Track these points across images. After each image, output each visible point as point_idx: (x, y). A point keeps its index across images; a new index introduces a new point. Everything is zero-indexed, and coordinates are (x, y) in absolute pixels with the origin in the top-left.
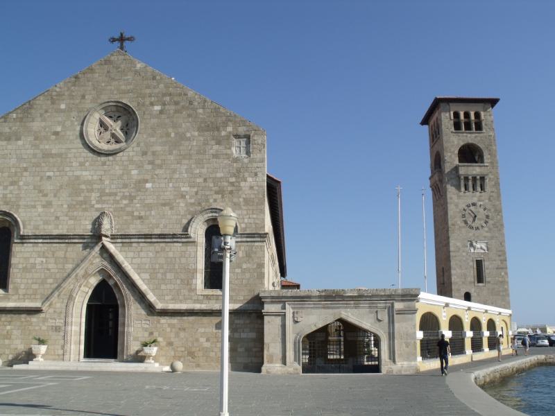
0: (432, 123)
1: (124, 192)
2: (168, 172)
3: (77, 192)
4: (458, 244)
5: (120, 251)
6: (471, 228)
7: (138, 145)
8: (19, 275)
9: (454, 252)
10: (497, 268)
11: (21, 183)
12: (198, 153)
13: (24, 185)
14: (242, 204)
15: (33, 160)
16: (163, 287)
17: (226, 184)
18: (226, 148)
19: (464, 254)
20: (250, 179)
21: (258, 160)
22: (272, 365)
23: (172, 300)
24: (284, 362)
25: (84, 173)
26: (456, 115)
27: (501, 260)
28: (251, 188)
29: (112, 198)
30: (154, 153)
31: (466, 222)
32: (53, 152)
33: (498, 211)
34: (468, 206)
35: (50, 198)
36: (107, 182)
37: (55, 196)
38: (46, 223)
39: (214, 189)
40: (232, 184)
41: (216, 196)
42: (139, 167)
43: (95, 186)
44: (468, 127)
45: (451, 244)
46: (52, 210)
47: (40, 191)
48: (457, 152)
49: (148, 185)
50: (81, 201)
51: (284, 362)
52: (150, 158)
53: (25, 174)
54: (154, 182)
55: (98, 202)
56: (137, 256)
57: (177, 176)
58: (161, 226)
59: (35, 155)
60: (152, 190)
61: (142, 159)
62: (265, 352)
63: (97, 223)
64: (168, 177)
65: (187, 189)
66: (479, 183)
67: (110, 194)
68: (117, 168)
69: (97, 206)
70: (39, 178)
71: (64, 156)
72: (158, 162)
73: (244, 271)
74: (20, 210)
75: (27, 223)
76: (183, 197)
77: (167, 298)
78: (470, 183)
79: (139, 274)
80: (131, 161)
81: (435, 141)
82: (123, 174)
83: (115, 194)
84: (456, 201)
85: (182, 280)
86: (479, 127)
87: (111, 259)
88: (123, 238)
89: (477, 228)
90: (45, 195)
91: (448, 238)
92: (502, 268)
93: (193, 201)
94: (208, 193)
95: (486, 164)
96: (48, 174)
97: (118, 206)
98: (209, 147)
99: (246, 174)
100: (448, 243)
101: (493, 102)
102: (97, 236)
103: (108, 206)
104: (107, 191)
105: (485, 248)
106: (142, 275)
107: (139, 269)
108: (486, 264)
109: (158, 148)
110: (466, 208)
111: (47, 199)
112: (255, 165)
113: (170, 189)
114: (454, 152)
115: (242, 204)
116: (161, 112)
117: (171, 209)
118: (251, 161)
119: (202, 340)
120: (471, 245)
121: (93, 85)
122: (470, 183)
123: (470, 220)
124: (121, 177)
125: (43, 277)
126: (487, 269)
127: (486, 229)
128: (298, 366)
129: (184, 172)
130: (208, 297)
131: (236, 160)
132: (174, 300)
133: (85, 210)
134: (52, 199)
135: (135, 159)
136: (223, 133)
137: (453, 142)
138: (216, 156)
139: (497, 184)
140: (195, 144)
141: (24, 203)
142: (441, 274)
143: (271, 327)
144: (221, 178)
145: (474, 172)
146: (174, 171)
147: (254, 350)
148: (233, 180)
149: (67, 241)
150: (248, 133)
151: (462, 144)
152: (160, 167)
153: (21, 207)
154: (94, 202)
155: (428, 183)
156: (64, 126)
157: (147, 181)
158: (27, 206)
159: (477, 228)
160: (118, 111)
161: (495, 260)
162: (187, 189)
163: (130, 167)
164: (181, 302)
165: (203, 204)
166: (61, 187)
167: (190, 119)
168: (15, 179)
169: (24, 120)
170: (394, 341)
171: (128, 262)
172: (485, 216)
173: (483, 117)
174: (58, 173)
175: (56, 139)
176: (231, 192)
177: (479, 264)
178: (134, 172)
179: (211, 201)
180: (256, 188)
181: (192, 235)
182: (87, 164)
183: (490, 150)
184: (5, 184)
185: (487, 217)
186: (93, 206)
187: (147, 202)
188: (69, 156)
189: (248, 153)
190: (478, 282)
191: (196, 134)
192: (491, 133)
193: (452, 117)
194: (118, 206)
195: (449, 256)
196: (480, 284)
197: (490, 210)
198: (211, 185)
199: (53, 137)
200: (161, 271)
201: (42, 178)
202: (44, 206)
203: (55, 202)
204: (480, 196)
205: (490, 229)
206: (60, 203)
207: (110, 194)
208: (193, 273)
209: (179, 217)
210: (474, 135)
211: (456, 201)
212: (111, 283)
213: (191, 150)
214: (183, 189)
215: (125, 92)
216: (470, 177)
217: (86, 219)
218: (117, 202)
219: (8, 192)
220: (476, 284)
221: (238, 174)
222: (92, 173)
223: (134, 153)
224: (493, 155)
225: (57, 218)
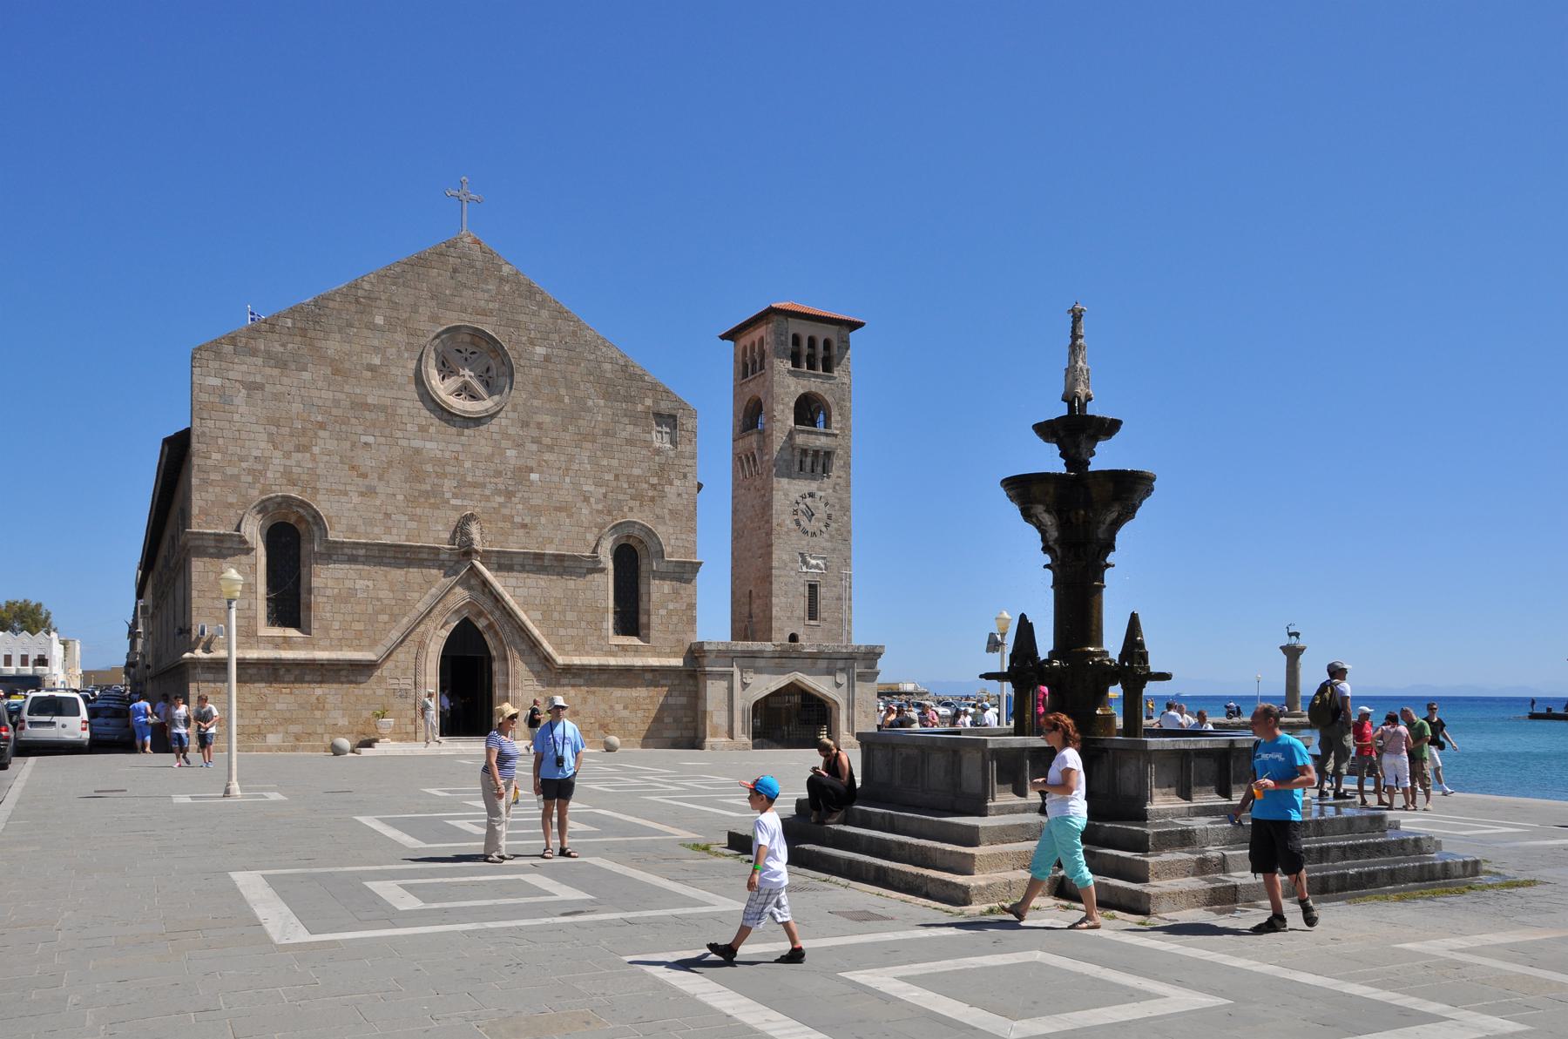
0: (746, 340)
1: (496, 484)
2: (562, 459)
3: (416, 476)
4: (785, 557)
5: (495, 577)
7: (514, 411)
8: (328, 608)
9: (778, 568)
11: (316, 450)
12: (606, 433)
13: (322, 453)
14: (667, 517)
15: (335, 411)
16: (562, 632)
17: (646, 486)
18: (644, 431)
19: (793, 573)
20: (677, 482)
21: (687, 454)
22: (716, 740)
23: (576, 650)
24: (731, 736)
25: (429, 445)
26: (796, 339)
28: (679, 495)
29: (477, 491)
30: (539, 426)
31: (798, 524)
32: (369, 401)
33: (846, 509)
34: (803, 497)
35: (373, 480)
36: (468, 464)
37: (380, 478)
38: (370, 522)
39: (629, 491)
40: (653, 486)
41: (632, 503)
42: (519, 446)
43: (449, 469)
45: (774, 556)
46: (378, 503)
47: (353, 468)
48: (792, 405)
49: (534, 477)
50: (427, 492)
51: (731, 736)
52: (535, 433)
53: (322, 433)
54: (541, 473)
55: (455, 496)
56: (522, 585)
57: (576, 467)
58: (556, 541)
59: (337, 403)
60: (540, 483)
61: (521, 433)
62: (708, 722)
63: (461, 528)
64: (563, 467)
65: (592, 488)
66: (817, 463)
67: (474, 485)
68: (483, 442)
69: (453, 502)
70: (347, 445)
71: (389, 411)
72: (547, 441)
73: (670, 614)
74: (319, 497)
75: (334, 520)
76: (586, 500)
77: (568, 648)
78: (809, 460)
79: (525, 612)
80: (506, 436)
81: (750, 378)
82: (493, 455)
83: (483, 485)
84: (786, 486)
85: (588, 623)
86: (828, 368)
87: (485, 583)
88: (505, 562)
89: (814, 534)
90: (364, 476)
91: (771, 545)
93: (600, 507)
94: (621, 497)
96: (364, 439)
97: (489, 505)
98: (621, 426)
99: (672, 475)
100: (770, 554)
101: (855, 326)
102: (467, 552)
103: (471, 503)
104: (469, 479)
105: (823, 566)
106: (531, 612)
107: (526, 605)
109: (547, 419)
110: (800, 500)
111: (367, 482)
112: (684, 462)
113: (566, 486)
114: (787, 404)
115: (667, 517)
116: (547, 358)
117: (570, 516)
118: (680, 455)
119: (619, 707)
120: (805, 562)
121: (430, 290)
123: (804, 522)
124: (490, 458)
125: (370, 610)
126: (824, 599)
128: (747, 740)
129: (586, 461)
130: (624, 649)
131: (658, 452)
132: (579, 651)
133: (435, 507)
134: (375, 482)
135: (512, 431)
136: (640, 408)
137: (789, 387)
138: (630, 442)
139: (847, 465)
140: (599, 419)
141: (327, 485)
143: (715, 691)
144: (638, 476)
145: (818, 443)
146: (571, 458)
147: (685, 720)
148: (654, 480)
149: (408, 555)
150: (673, 412)
151: (801, 391)
152: (550, 448)
153: (321, 492)
154: (448, 495)
156: (384, 357)
157: (531, 470)
158: (332, 491)
159: (814, 534)
160: (473, 343)
161: (835, 586)
162: (592, 488)
163: (504, 444)
164: (588, 654)
165: (615, 513)
166: (390, 463)
167: (592, 378)
168: (304, 441)
169: (311, 334)
170: (853, 709)
171: (508, 593)
172: (825, 516)
173: (835, 350)
174: (382, 440)
175: (373, 378)
176: (652, 499)
178: (511, 453)
179: (626, 509)
180: (685, 496)
181: (602, 558)
182: (432, 430)
183: (841, 408)
184: (286, 449)
186: (448, 502)
187: (533, 502)
188: (400, 411)
189: (673, 442)
191: (602, 402)
192: (846, 380)
193: (790, 345)
194: (489, 505)
195: (770, 575)
198: (625, 486)
199: (369, 374)
200: (559, 608)
201: (353, 445)
202: (362, 494)
203: (381, 488)
205: (832, 536)
206: (390, 491)
207: (474, 485)
208: (603, 613)
209: (582, 530)
211: (786, 486)
212: (481, 624)
213: (594, 427)
214: (585, 488)
215: (484, 313)
217: (437, 522)
218: (487, 499)
219: (294, 463)
221: (661, 471)
222: (442, 445)
223: (509, 422)
224: (844, 416)
225: (388, 516)
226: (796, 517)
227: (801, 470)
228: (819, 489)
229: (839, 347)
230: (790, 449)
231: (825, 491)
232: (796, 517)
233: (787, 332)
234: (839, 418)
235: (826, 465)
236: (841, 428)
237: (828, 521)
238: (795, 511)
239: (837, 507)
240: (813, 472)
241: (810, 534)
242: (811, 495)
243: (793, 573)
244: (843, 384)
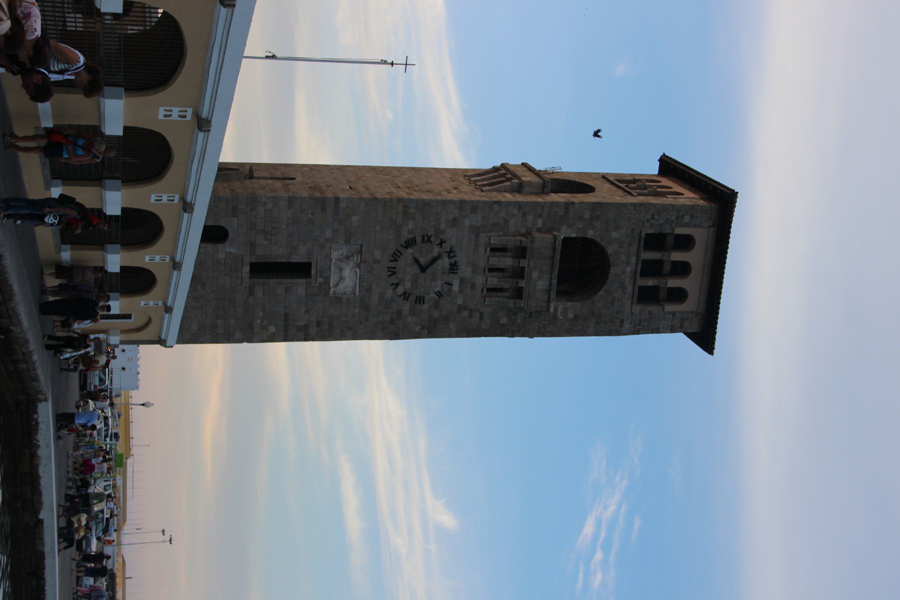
0: (665, 182)
4: (355, 219)
6: (396, 257)
10: (286, 316)
19: (328, 234)
26: (685, 243)
31: (410, 243)
34: (451, 253)
44: (650, 269)
48: (590, 234)
78: (507, 262)
84: (467, 223)
86: (647, 296)
89: (392, 272)
92: (286, 329)
95: (552, 305)
108: (300, 286)
122: (507, 262)
126: (287, 290)
127: (390, 292)
142: (278, 174)
145: (535, 275)
151: (610, 250)
155: (514, 160)
159: (392, 272)
161: (307, 312)
173: (670, 308)
177: (302, 270)
185: (420, 300)
190: (252, 264)
193: (679, 231)
196: (247, 269)
197: (436, 305)
204: (473, 287)
210: (628, 282)
211: (467, 223)
216: (523, 263)
220: (248, 260)
226: (419, 239)
227: (492, 250)
228: (462, 281)
229: (674, 314)
230: (523, 230)
231: (461, 291)
232: (419, 239)
233: (695, 226)
234: (571, 316)
235: (500, 294)
236: (555, 318)
237: (412, 298)
238: (429, 238)
239: (436, 314)
240: (491, 270)
241: (392, 264)
242: (453, 268)
243: (328, 234)
244: (622, 321)
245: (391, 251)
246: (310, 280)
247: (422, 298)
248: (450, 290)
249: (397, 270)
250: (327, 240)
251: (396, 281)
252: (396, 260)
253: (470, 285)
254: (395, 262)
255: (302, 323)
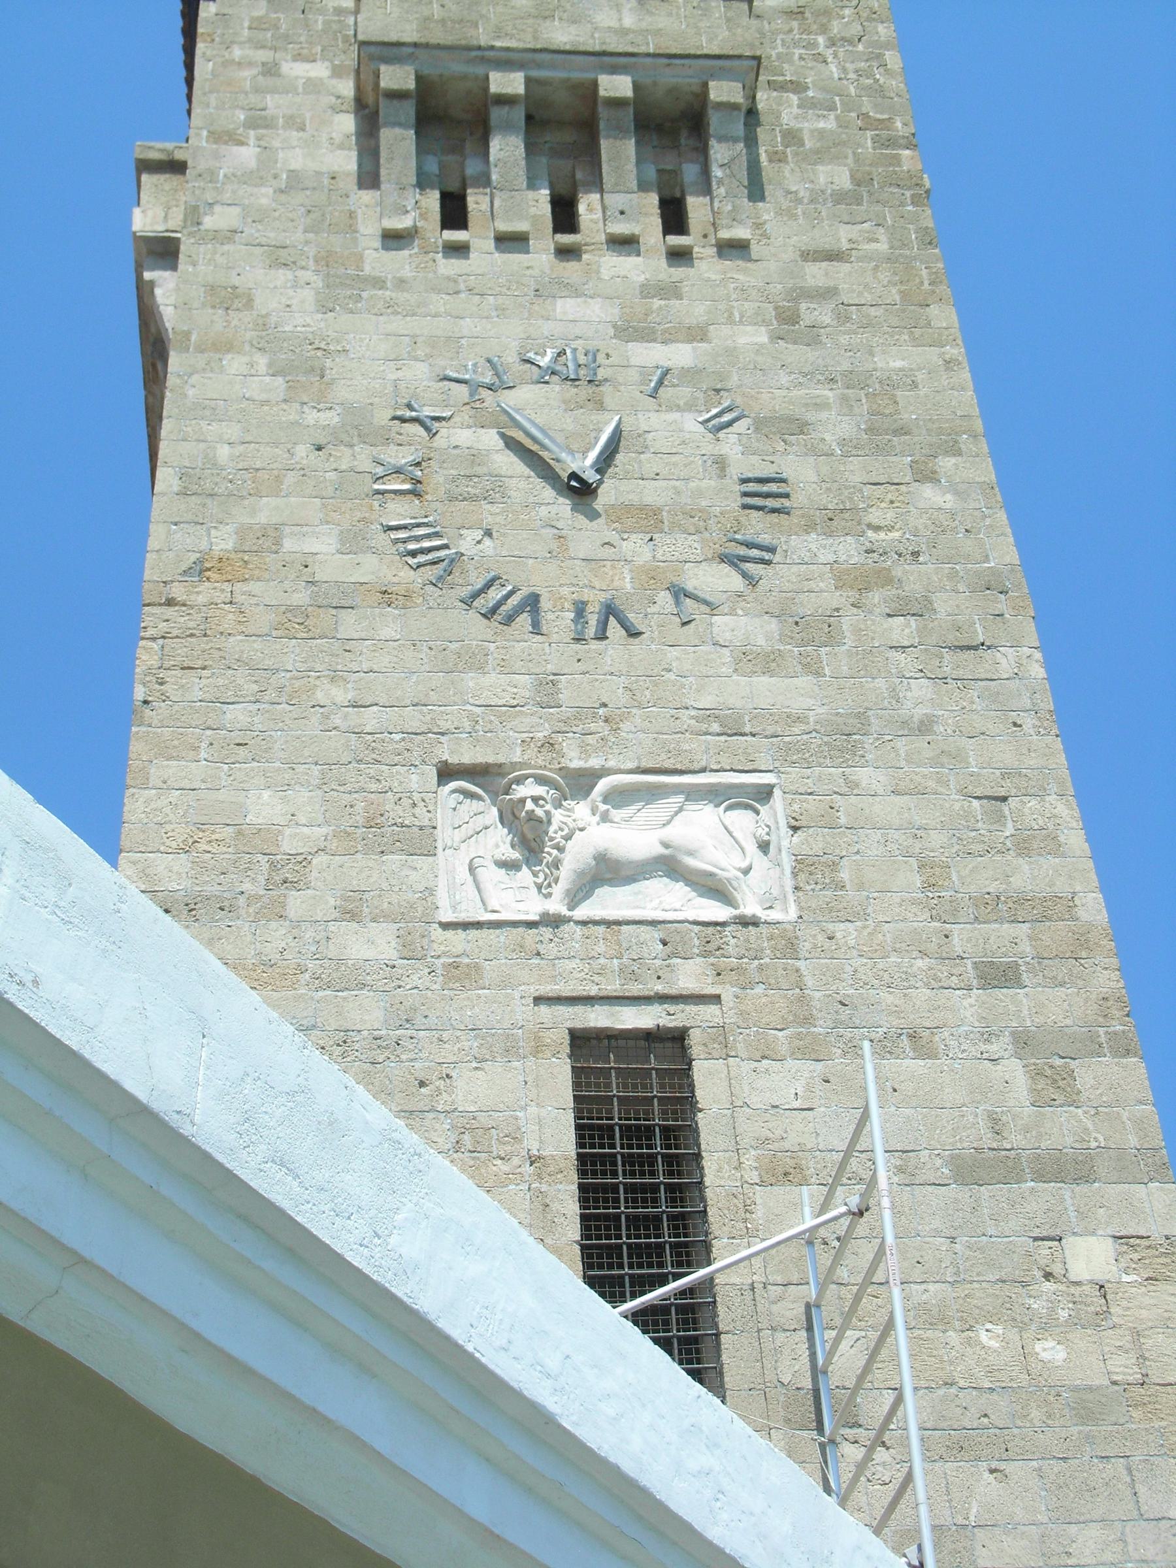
27: (1023, 1042)
231: (696, 334)
241: (559, 621)
245: (474, 626)
246: (695, 1039)
247: (752, 487)
248: (691, 374)
249: (595, 600)
250: (411, 951)
251: (665, 599)
252: (532, 603)
253: (657, 303)
254: (545, 604)
255: (1014, 1071)
